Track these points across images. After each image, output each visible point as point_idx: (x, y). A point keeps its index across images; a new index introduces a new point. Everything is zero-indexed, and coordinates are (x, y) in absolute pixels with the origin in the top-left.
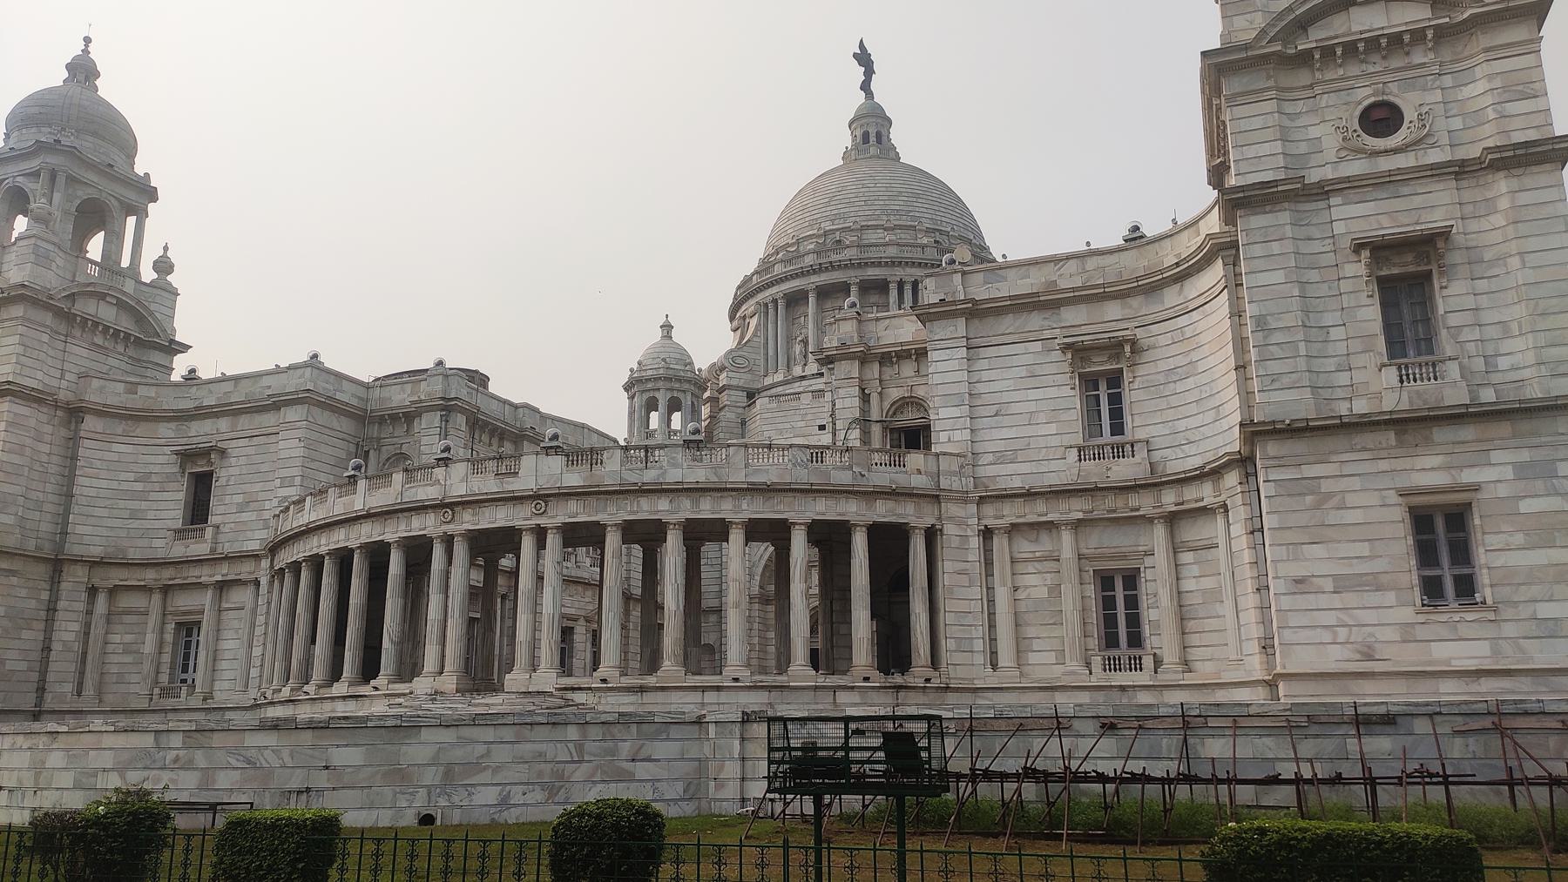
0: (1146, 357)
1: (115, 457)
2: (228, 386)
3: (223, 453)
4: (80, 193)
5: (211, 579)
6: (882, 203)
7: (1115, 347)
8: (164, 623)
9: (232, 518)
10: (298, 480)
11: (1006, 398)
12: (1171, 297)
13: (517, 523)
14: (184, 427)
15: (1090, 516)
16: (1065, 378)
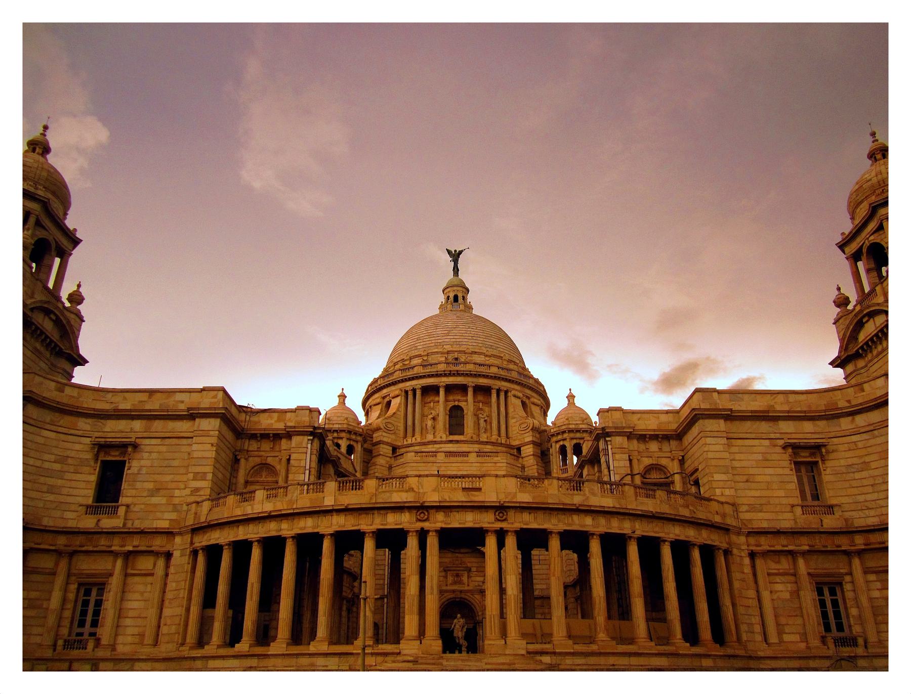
0: (832, 456)
1: (41, 440)
2: (144, 397)
3: (135, 446)
4: (37, 233)
5: (123, 549)
6: (482, 339)
7: (816, 448)
8: (67, 583)
9: (143, 500)
10: (210, 476)
11: (752, 471)
12: (845, 423)
13: (485, 525)
14: (100, 424)
15: (813, 549)
16: (786, 464)
